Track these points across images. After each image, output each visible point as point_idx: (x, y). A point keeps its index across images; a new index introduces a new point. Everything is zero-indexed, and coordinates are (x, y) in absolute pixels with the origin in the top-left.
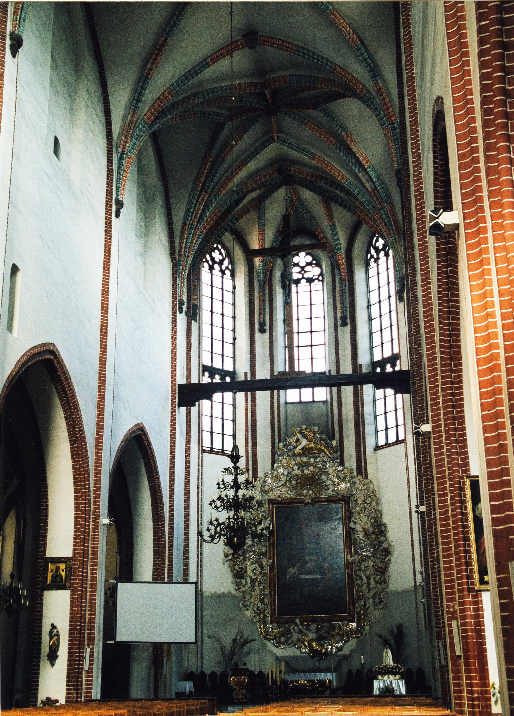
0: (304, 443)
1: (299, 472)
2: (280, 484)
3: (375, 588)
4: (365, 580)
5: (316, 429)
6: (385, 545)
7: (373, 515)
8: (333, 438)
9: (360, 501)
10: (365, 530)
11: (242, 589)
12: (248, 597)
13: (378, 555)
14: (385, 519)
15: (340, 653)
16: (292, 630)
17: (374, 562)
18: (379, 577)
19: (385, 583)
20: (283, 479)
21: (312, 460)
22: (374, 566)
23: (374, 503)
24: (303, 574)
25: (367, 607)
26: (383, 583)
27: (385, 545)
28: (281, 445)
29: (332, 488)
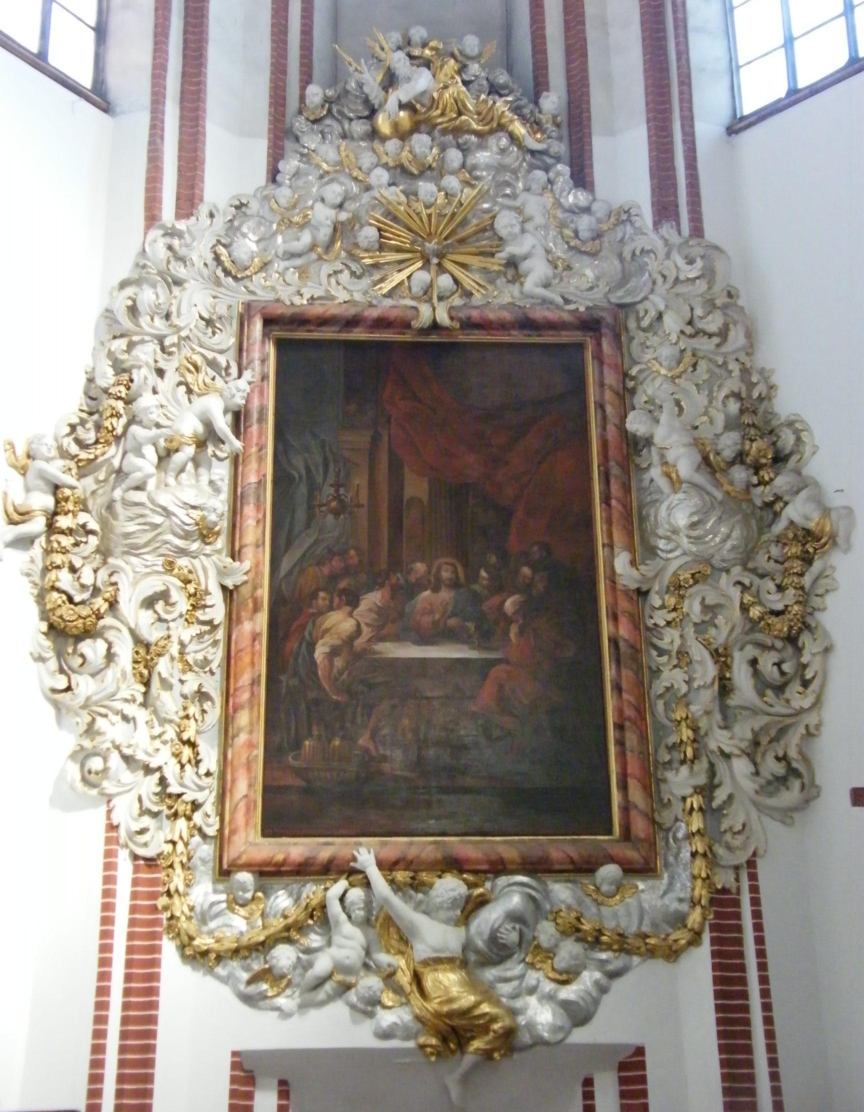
0: (422, 81)
1: (395, 195)
2: (306, 238)
3: (755, 712)
4: (708, 671)
5: (471, 43)
6: (797, 511)
7: (734, 384)
8: (540, 85)
9: (672, 323)
10: (697, 443)
11: (85, 686)
12: (112, 730)
13: (761, 561)
14: (785, 405)
15: (579, 1036)
16: (335, 908)
17: (745, 588)
18: (774, 657)
19: (806, 684)
20: (324, 215)
21: (454, 156)
22: (744, 608)
23: (737, 338)
24: (397, 638)
25: (720, 796)
26: (796, 686)
27: (797, 511)
28: (315, 94)
29: (537, 270)
